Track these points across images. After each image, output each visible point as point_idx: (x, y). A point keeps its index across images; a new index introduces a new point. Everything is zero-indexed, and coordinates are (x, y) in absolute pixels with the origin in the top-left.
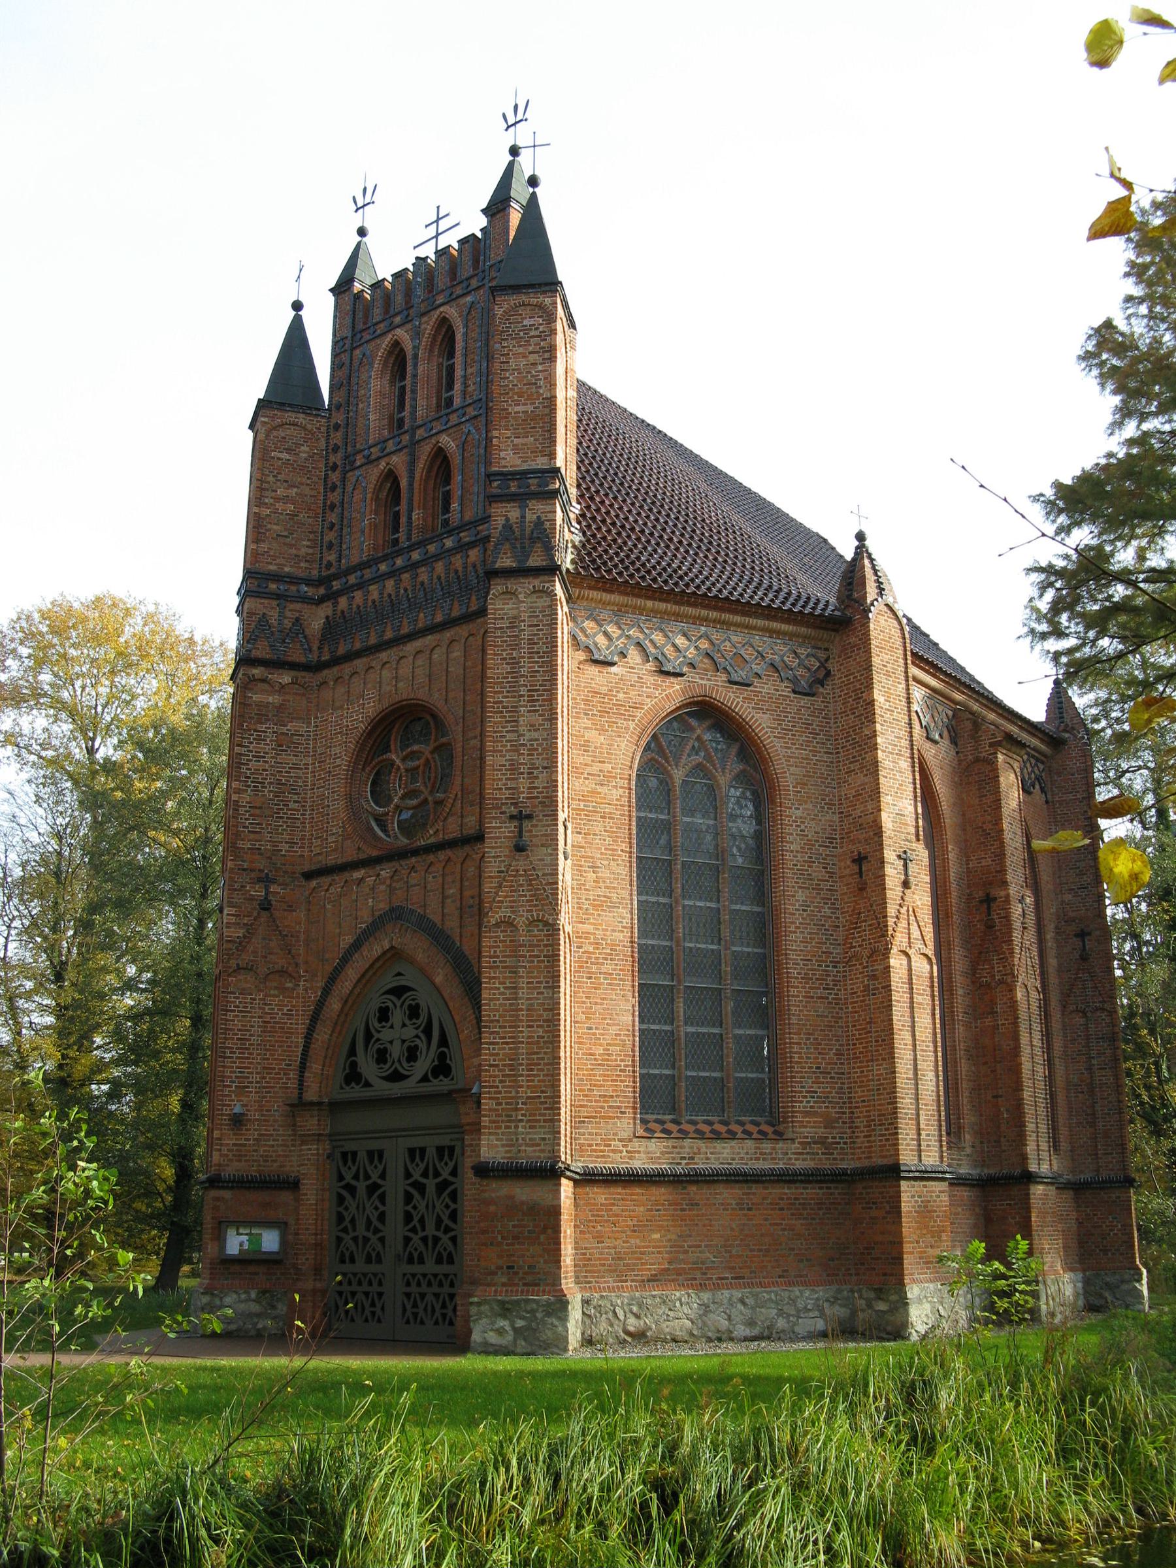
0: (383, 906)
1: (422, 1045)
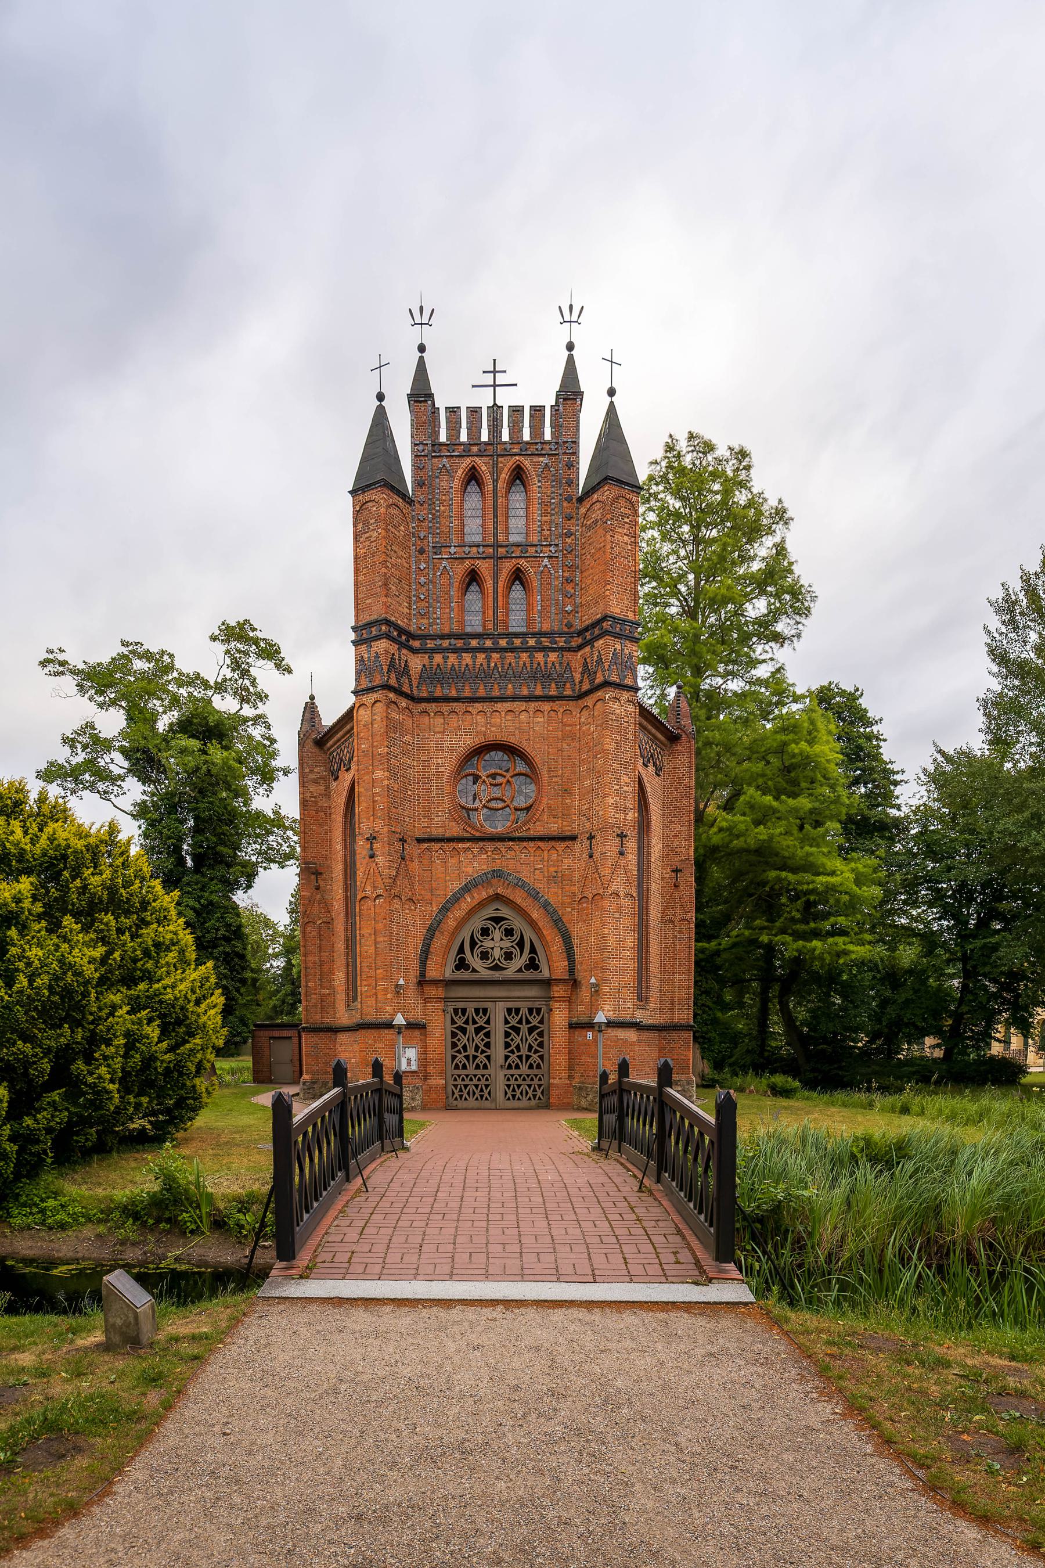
1: (516, 951)
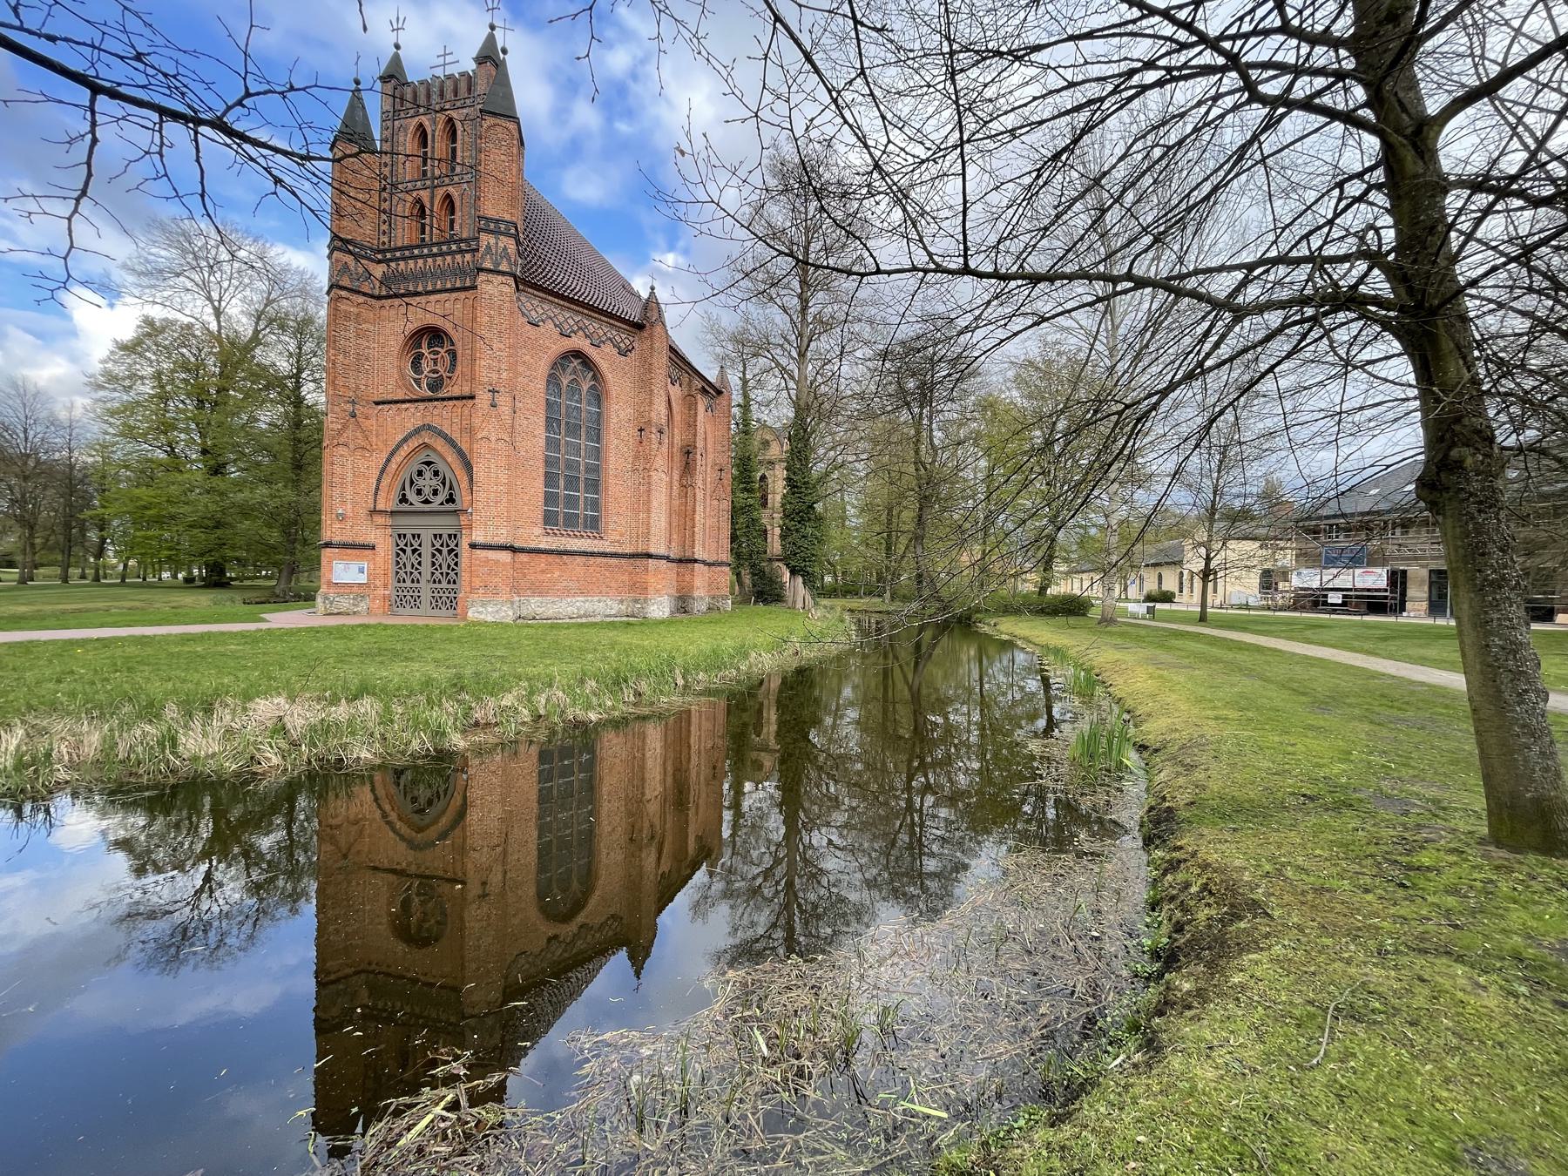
0: (420, 423)
1: (440, 488)
